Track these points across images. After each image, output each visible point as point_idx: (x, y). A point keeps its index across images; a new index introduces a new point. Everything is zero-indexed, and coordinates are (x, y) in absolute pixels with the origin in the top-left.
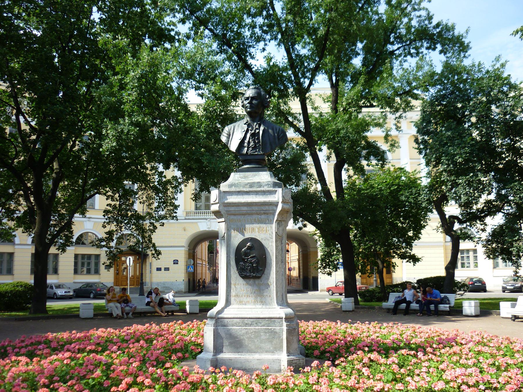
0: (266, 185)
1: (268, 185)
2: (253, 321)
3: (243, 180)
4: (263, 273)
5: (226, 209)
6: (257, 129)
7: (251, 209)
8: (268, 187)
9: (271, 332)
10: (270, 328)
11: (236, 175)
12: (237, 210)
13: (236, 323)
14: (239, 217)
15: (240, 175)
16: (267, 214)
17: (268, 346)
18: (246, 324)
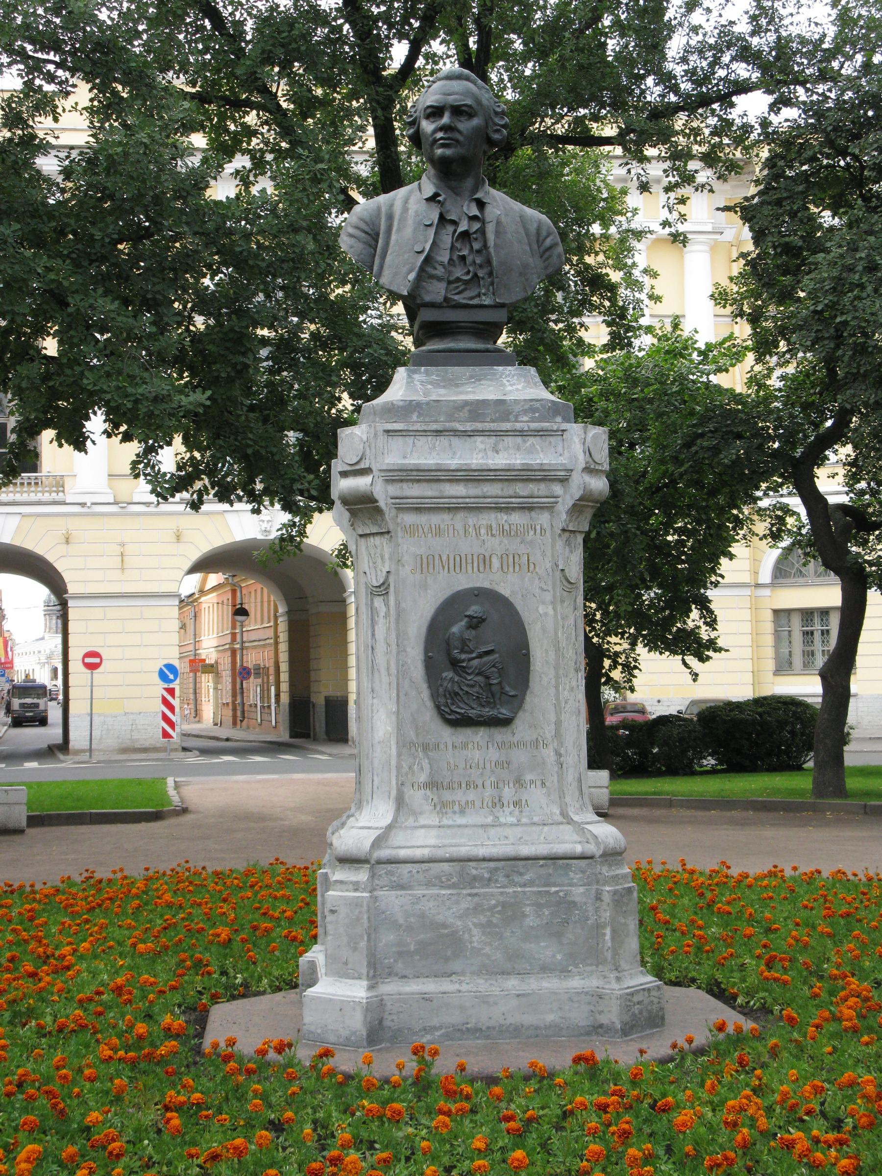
0: (525, 412)
1: (533, 410)
2: (496, 869)
3: (442, 391)
5: (393, 490)
6: (474, 218)
7: (511, 492)
8: (533, 420)
9: (559, 903)
10: (553, 889)
11: (417, 377)
12: (429, 493)
13: (438, 877)
14: (436, 519)
15: (427, 373)
16: (531, 509)
17: (547, 951)
18: (475, 878)
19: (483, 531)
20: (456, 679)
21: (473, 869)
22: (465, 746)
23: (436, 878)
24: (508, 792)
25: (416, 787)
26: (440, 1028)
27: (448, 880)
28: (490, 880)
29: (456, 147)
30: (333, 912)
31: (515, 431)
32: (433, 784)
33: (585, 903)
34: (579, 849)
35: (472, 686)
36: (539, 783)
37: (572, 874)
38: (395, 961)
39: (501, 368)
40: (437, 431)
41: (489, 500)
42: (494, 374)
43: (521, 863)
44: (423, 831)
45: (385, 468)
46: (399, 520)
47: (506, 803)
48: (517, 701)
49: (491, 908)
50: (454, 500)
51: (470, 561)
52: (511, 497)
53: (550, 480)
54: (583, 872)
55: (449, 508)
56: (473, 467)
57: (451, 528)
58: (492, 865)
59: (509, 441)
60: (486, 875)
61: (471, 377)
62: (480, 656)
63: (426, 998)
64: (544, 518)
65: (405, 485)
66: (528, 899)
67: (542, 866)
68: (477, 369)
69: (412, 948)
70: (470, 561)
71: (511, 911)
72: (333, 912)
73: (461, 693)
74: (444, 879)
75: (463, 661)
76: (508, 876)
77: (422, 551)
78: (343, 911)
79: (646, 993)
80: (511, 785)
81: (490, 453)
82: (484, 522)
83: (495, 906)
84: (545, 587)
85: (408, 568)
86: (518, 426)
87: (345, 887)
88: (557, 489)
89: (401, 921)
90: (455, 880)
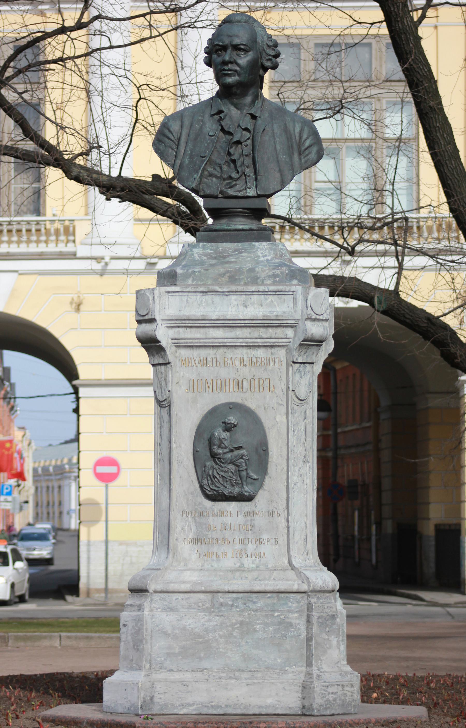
0: (269, 277)
2: (237, 599)
4: (261, 486)
5: (172, 333)
8: (274, 283)
9: (280, 623)
10: (276, 614)
12: (198, 336)
14: (203, 353)
15: (204, 247)
16: (272, 347)
18: (222, 604)
19: (237, 363)
20: (216, 467)
21: (221, 598)
22: (221, 513)
23: (195, 603)
24: (251, 547)
25: (186, 542)
26: (193, 704)
27: (203, 605)
28: (232, 606)
29: (234, 76)
30: (125, 625)
31: (259, 292)
32: (196, 540)
33: (299, 624)
34: (295, 587)
35: (225, 472)
36: (273, 541)
37: (290, 604)
38: (165, 659)
39: (257, 244)
40: (203, 292)
41: (241, 340)
42: (252, 248)
43: (254, 595)
44: (189, 572)
45: (166, 318)
46: (177, 354)
47: (249, 555)
48: (259, 483)
49: (233, 625)
50: (216, 341)
51: (227, 383)
52: (256, 339)
53: (284, 327)
54: (298, 602)
55: (213, 346)
56: (228, 317)
57: (214, 360)
58: (234, 595)
59: (255, 298)
60: (230, 603)
61: (235, 251)
62: (232, 451)
63: (184, 684)
64: (282, 353)
65: (181, 330)
66: (258, 620)
67: (269, 597)
68: (240, 244)
69: (177, 651)
70: (227, 383)
71: (246, 627)
72: (125, 625)
73: (218, 477)
74: (200, 604)
75: (220, 454)
76: (245, 604)
77: (195, 376)
78: (130, 625)
79: (340, 688)
80: (254, 542)
81: (241, 308)
82: (239, 356)
83: (236, 624)
84: (281, 403)
85: (184, 388)
86: (262, 288)
87: (133, 609)
88: (290, 332)
89: (170, 632)
90: (208, 605)
